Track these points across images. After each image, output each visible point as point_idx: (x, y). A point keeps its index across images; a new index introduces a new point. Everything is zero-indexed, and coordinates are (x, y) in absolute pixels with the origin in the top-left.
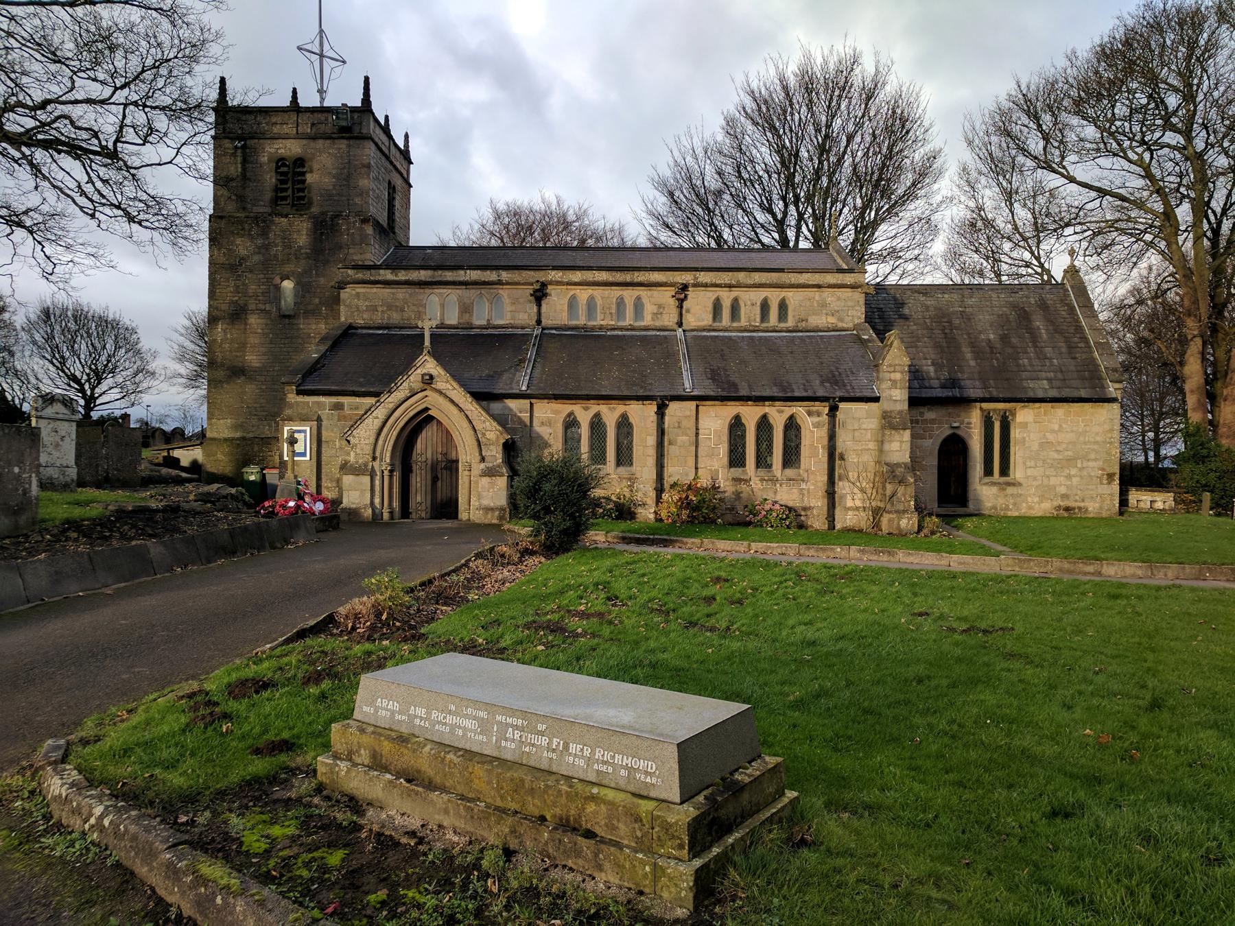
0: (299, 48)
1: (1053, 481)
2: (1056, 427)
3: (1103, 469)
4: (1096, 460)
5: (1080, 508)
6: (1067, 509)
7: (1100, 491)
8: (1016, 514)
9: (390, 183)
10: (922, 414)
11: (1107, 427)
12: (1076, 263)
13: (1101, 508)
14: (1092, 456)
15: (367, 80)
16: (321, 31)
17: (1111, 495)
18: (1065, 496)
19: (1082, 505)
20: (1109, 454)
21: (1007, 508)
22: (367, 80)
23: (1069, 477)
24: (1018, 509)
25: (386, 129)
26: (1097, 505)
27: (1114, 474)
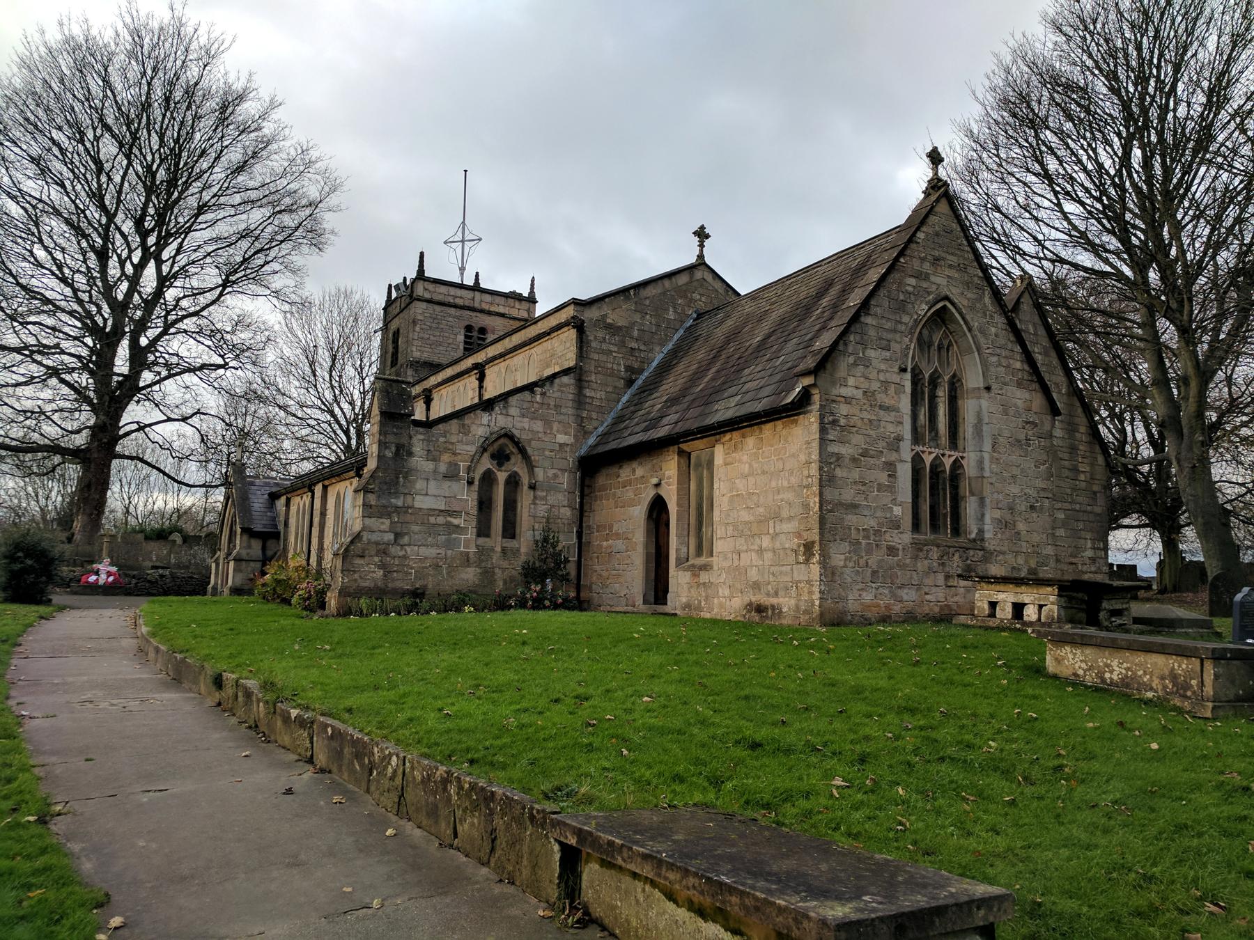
0: (445, 243)
1: (746, 559)
2: (746, 469)
3: (799, 535)
4: (790, 518)
5: (773, 607)
6: (760, 609)
7: (796, 577)
8: (708, 616)
9: (469, 328)
10: (634, 471)
11: (802, 458)
12: (942, 173)
13: (797, 607)
14: (785, 514)
15: (422, 255)
16: (463, 223)
17: (809, 582)
18: (756, 586)
19: (774, 601)
20: (806, 507)
21: (699, 608)
22: (422, 255)
23: (761, 551)
24: (711, 610)
25: (476, 287)
26: (793, 602)
27: (813, 543)
